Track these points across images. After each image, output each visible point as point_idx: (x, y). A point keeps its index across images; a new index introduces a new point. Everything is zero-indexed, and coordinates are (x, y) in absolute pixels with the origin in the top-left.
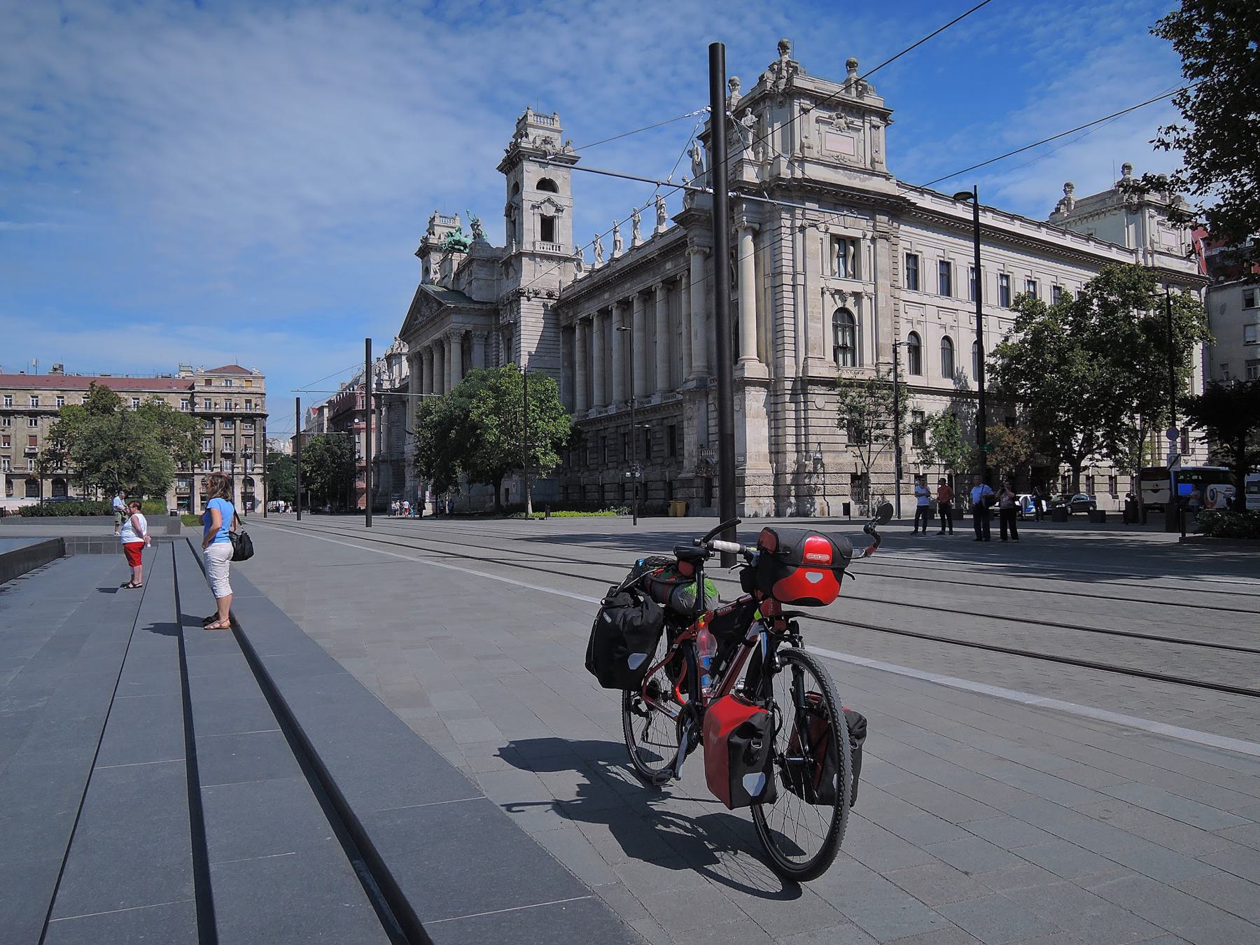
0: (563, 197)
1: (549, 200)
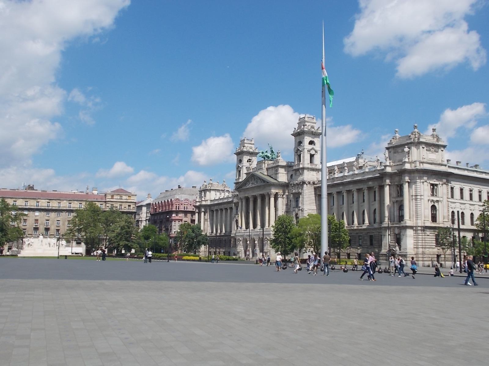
0: (317, 147)
1: (313, 148)
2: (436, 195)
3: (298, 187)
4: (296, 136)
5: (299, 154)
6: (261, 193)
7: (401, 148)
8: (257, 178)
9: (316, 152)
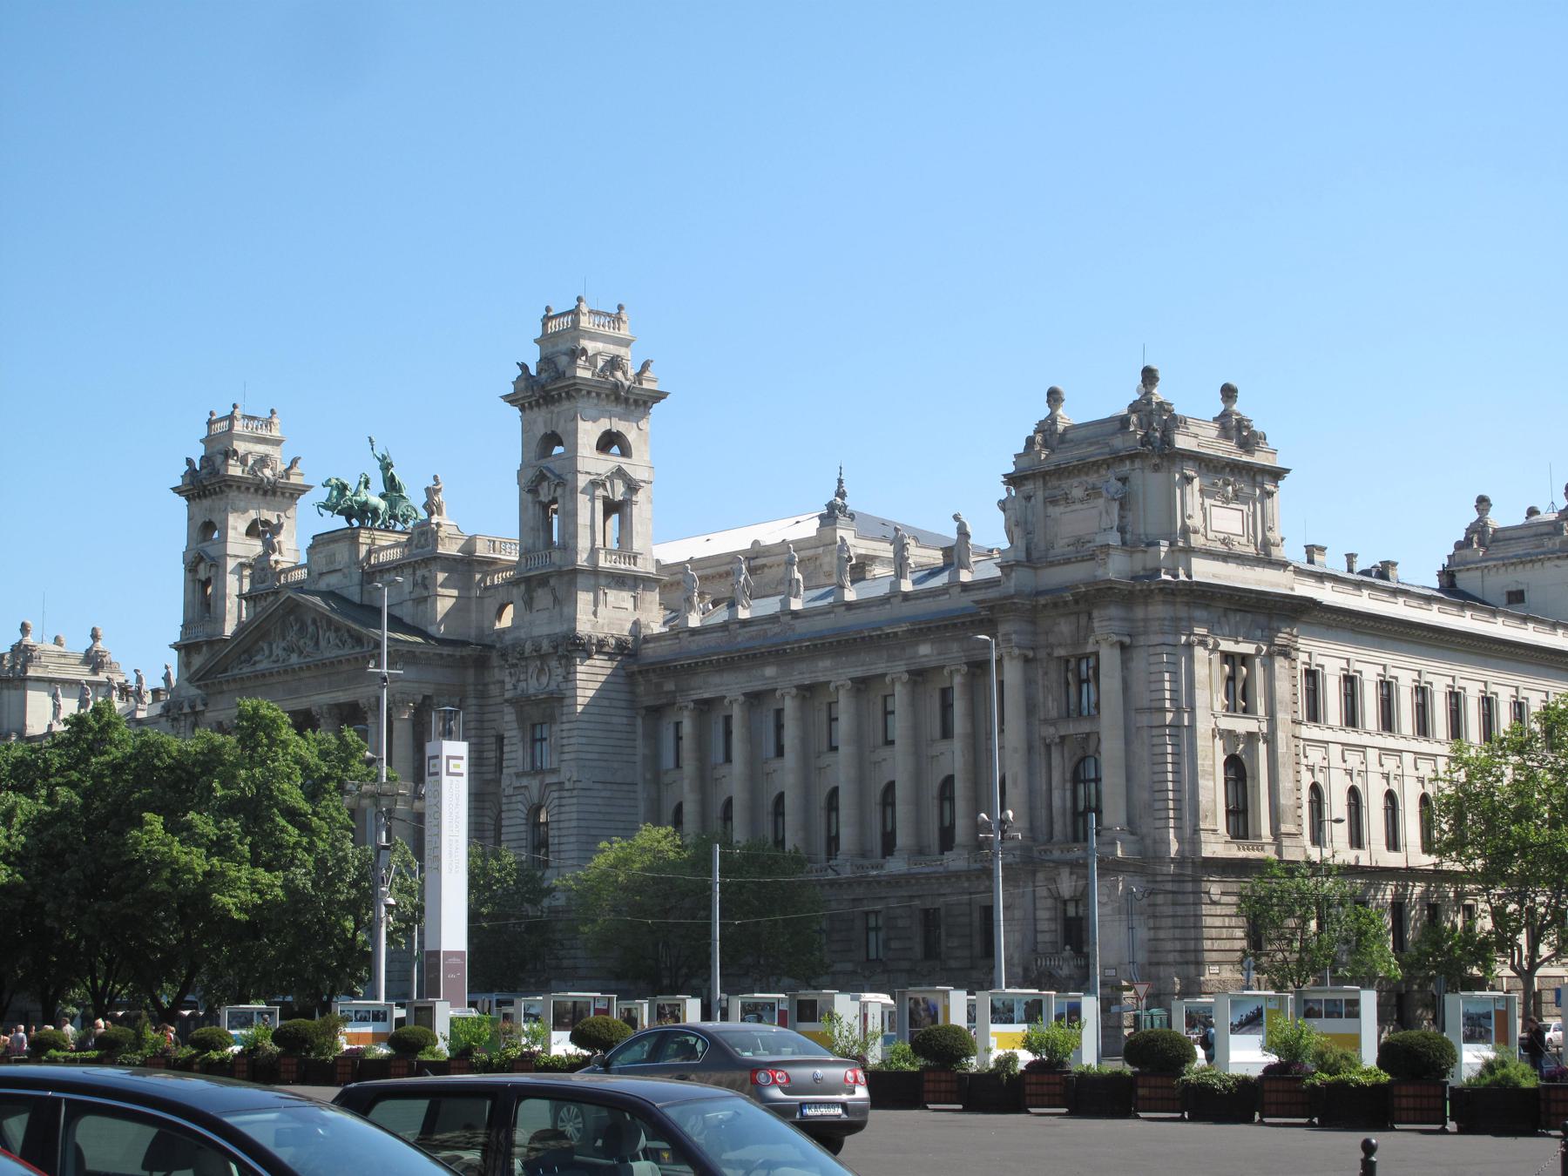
3: (541, 671)
4: (531, 407)
5: (544, 498)
6: (342, 697)
7: (1084, 478)
8: (314, 622)
9: (632, 487)
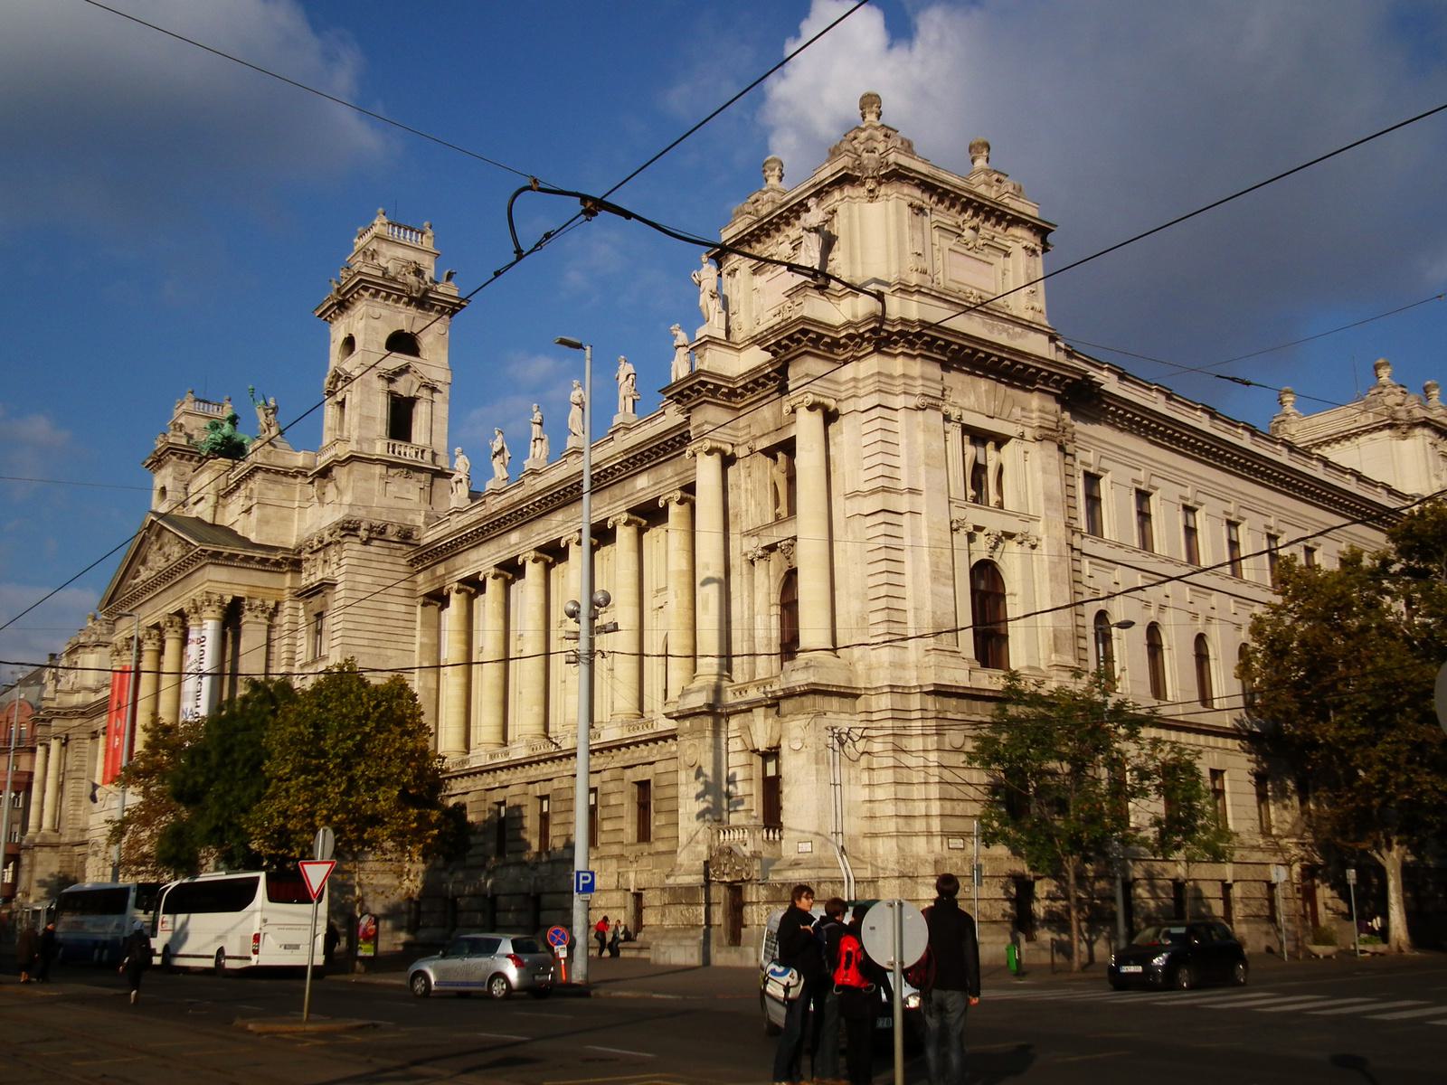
2: (1001, 505)
